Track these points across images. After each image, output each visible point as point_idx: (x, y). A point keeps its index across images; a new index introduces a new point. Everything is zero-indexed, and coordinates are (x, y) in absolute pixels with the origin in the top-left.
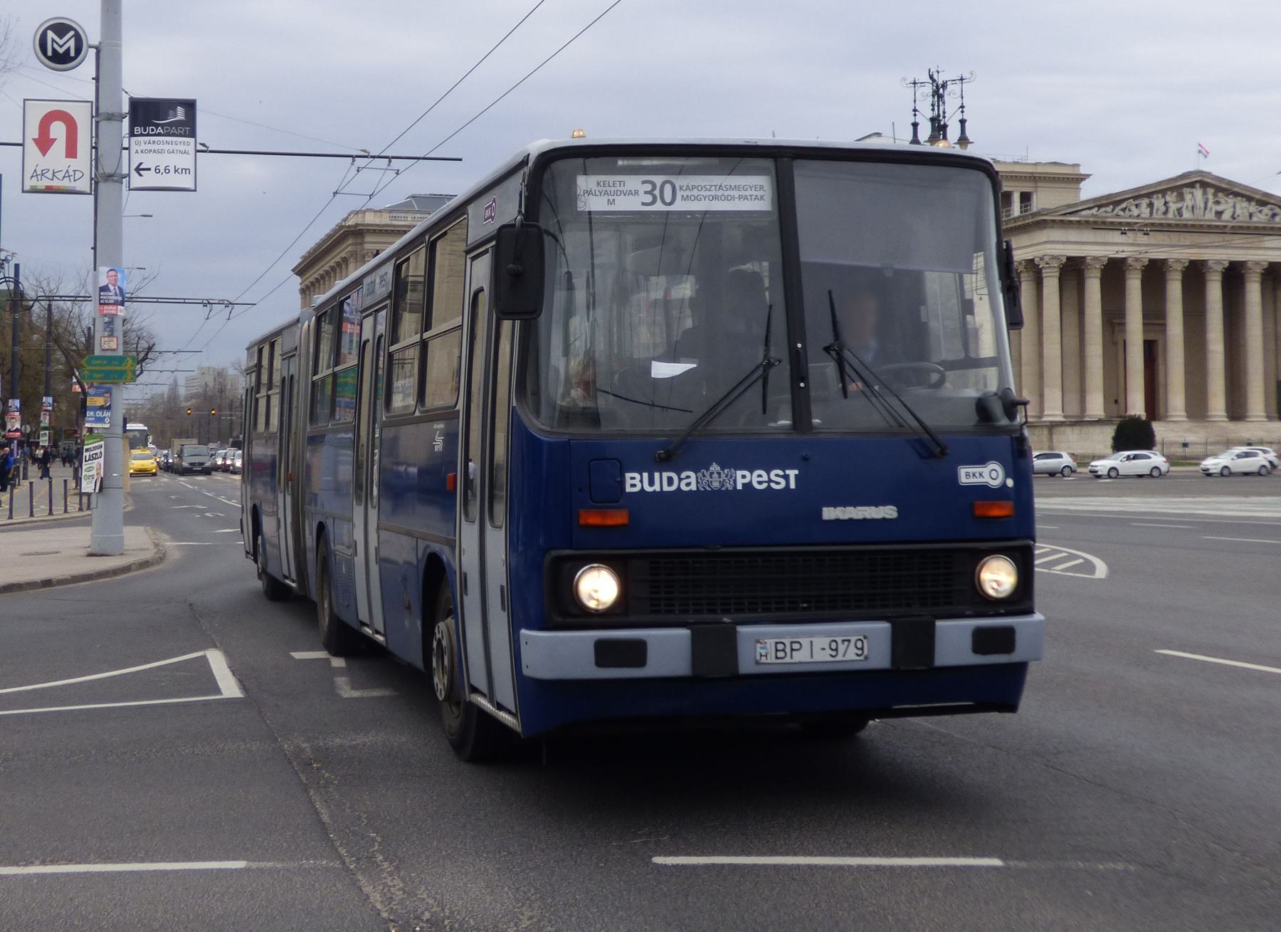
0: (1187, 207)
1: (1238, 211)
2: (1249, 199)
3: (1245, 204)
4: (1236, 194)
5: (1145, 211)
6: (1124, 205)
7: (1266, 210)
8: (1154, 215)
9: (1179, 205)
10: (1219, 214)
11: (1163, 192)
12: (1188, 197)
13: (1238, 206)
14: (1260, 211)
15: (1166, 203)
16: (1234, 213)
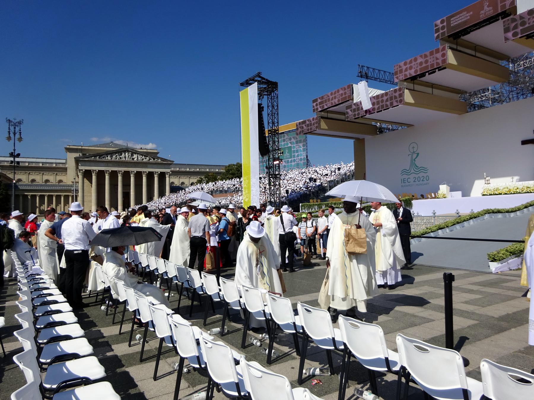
0: (123, 157)
1: (139, 158)
2: (142, 155)
3: (141, 156)
4: (138, 154)
5: (109, 158)
6: (103, 156)
7: (147, 158)
8: (113, 159)
9: (120, 156)
10: (133, 159)
11: (116, 153)
12: (123, 154)
13: (139, 157)
14: (146, 159)
15: (116, 156)
16: (138, 158)
